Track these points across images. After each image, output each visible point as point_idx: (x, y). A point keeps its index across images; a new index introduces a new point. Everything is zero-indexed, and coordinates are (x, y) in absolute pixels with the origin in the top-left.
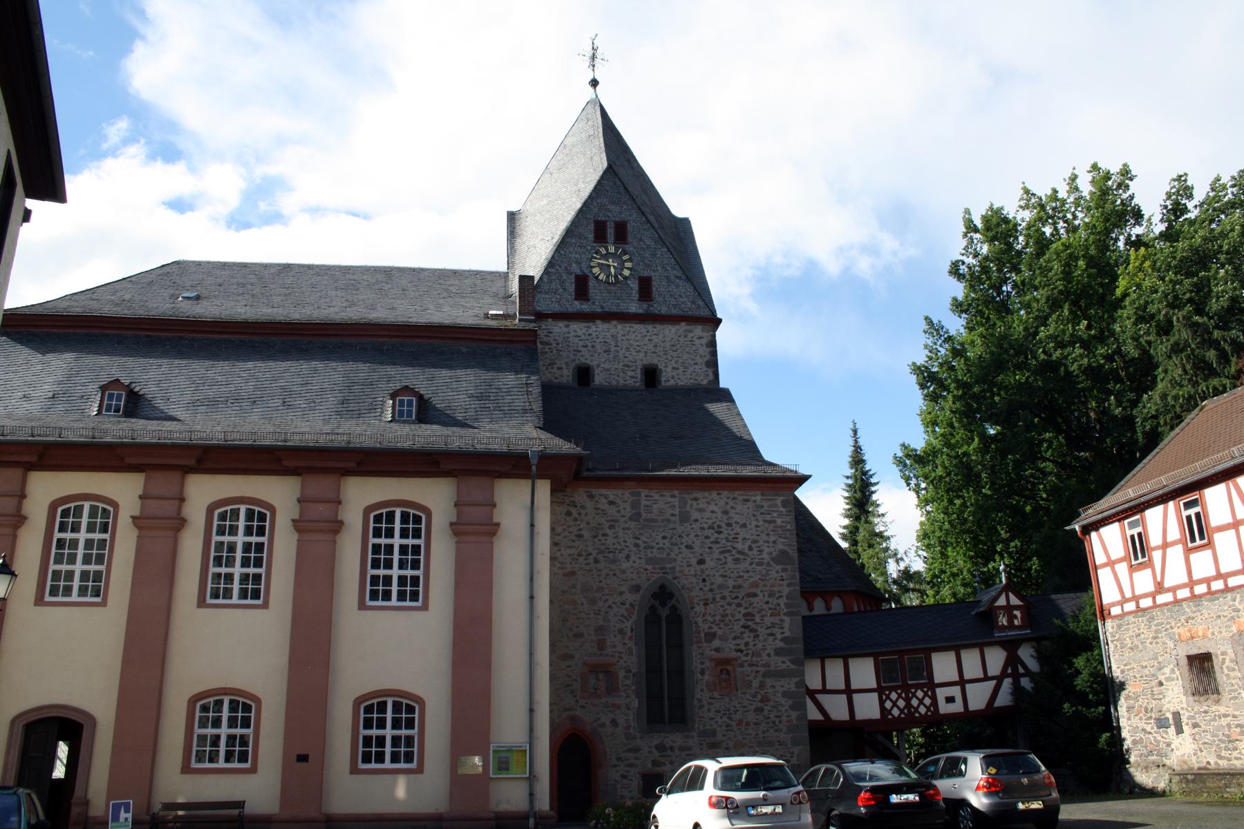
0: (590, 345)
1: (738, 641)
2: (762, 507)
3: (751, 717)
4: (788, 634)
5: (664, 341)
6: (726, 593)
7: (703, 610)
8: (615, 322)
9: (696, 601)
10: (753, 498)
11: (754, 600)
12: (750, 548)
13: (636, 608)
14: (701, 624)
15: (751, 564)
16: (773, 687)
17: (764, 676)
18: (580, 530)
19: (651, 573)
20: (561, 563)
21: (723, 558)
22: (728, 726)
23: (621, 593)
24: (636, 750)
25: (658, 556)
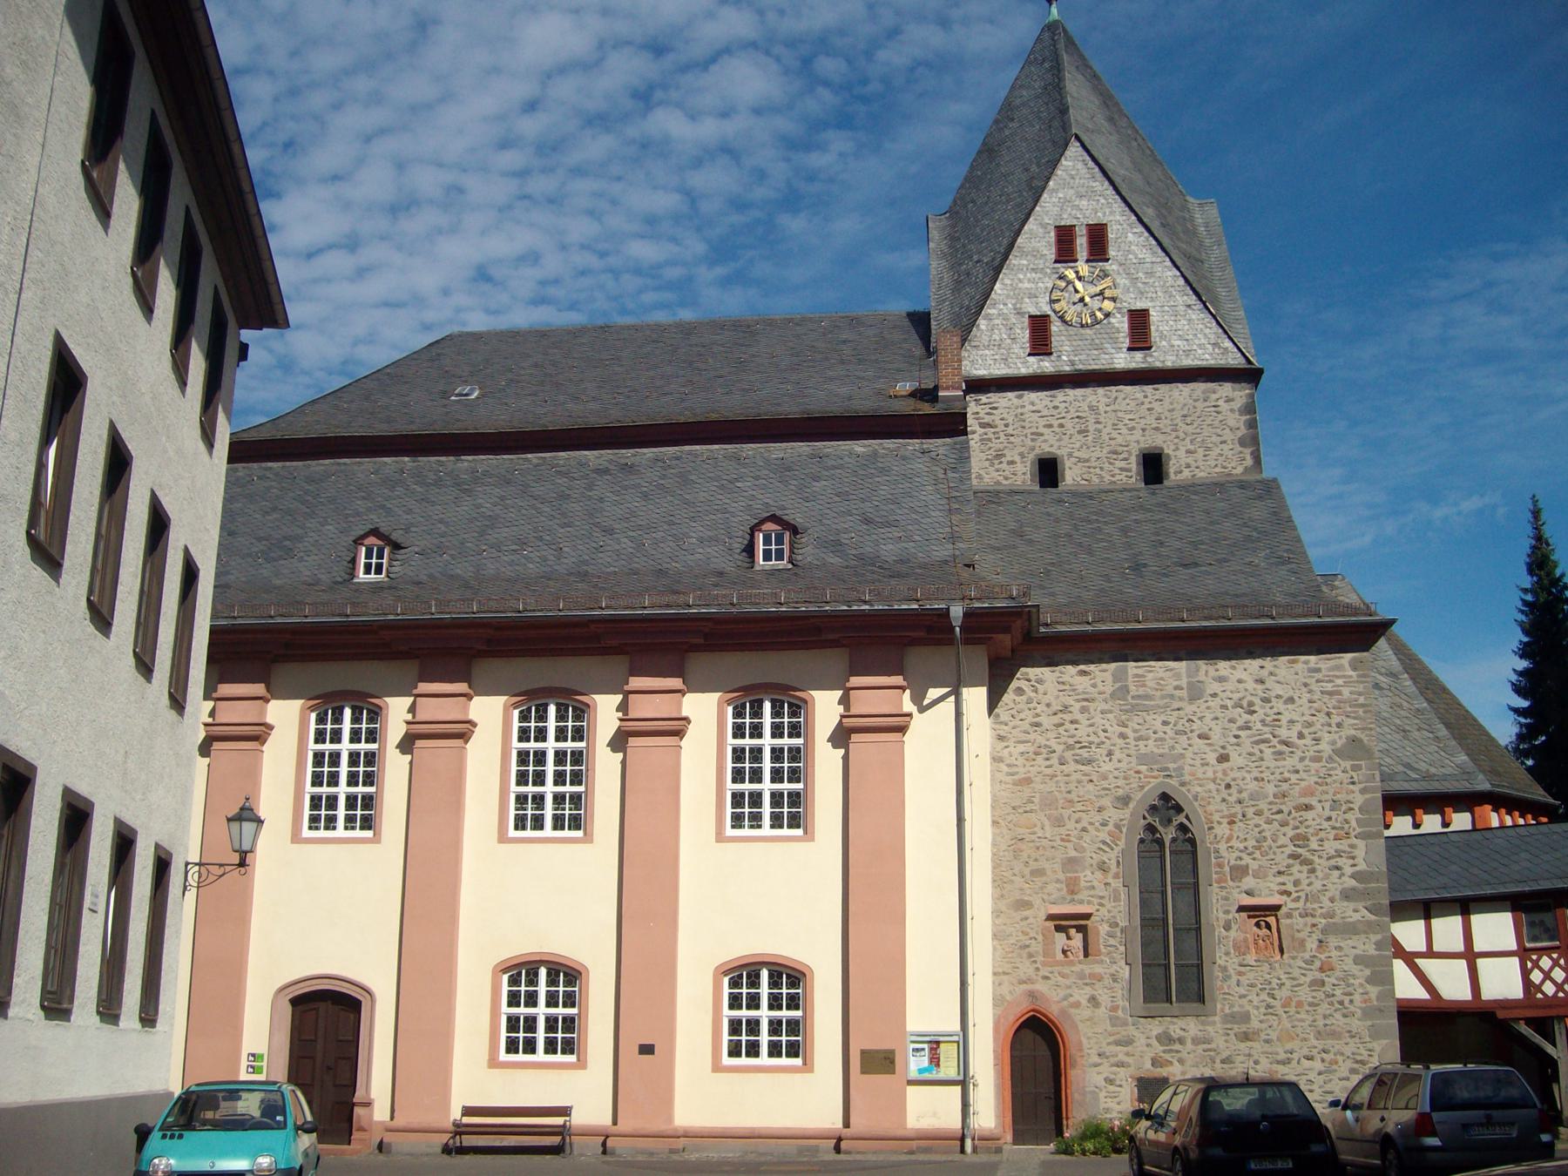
2: (1318, 670)
3: (1305, 994)
4: (1362, 866)
6: (1263, 805)
7: (1228, 832)
9: (1216, 817)
11: (1309, 815)
12: (1301, 736)
13: (1124, 830)
14: (1224, 852)
15: (1302, 759)
16: (1339, 948)
17: (1324, 931)
18: (1038, 715)
22: (1269, 1006)
24: (1128, 1042)
25: (1156, 750)
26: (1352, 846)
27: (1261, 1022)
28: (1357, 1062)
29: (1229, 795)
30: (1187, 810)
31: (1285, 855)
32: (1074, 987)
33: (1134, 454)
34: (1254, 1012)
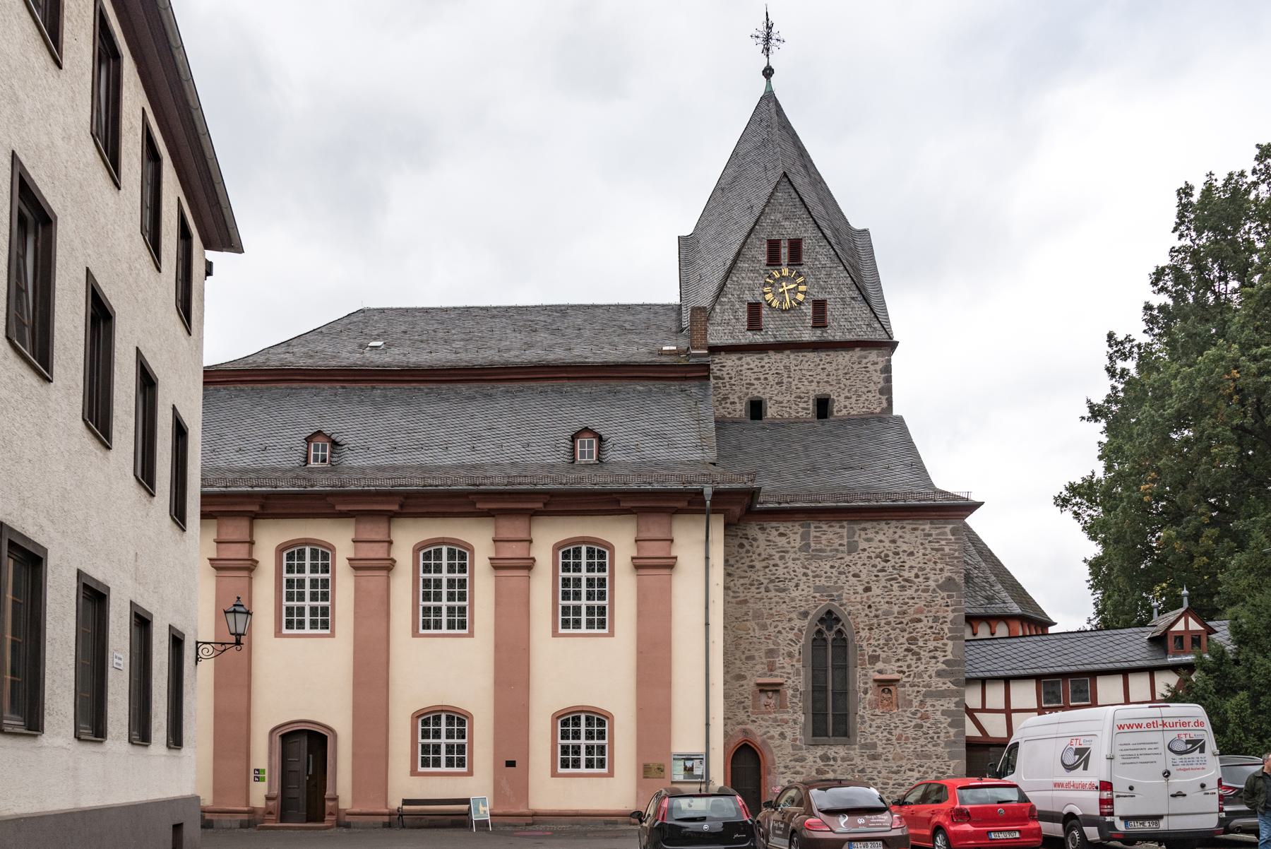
0: (762, 377)
1: (899, 664)
2: (930, 535)
3: (910, 732)
4: (950, 657)
5: (838, 369)
6: (891, 619)
7: (868, 635)
8: (788, 352)
9: (861, 626)
10: (922, 527)
11: (919, 625)
12: (917, 576)
13: (804, 633)
14: (865, 647)
15: (917, 591)
16: (933, 706)
17: (925, 695)
18: (752, 561)
19: (819, 600)
20: (734, 592)
21: (889, 586)
22: (888, 740)
23: (790, 620)
24: (802, 759)
26: (945, 645)
27: (883, 748)
28: (940, 773)
29: (871, 612)
30: (843, 620)
31: (903, 650)
33: (811, 398)
34: (879, 743)
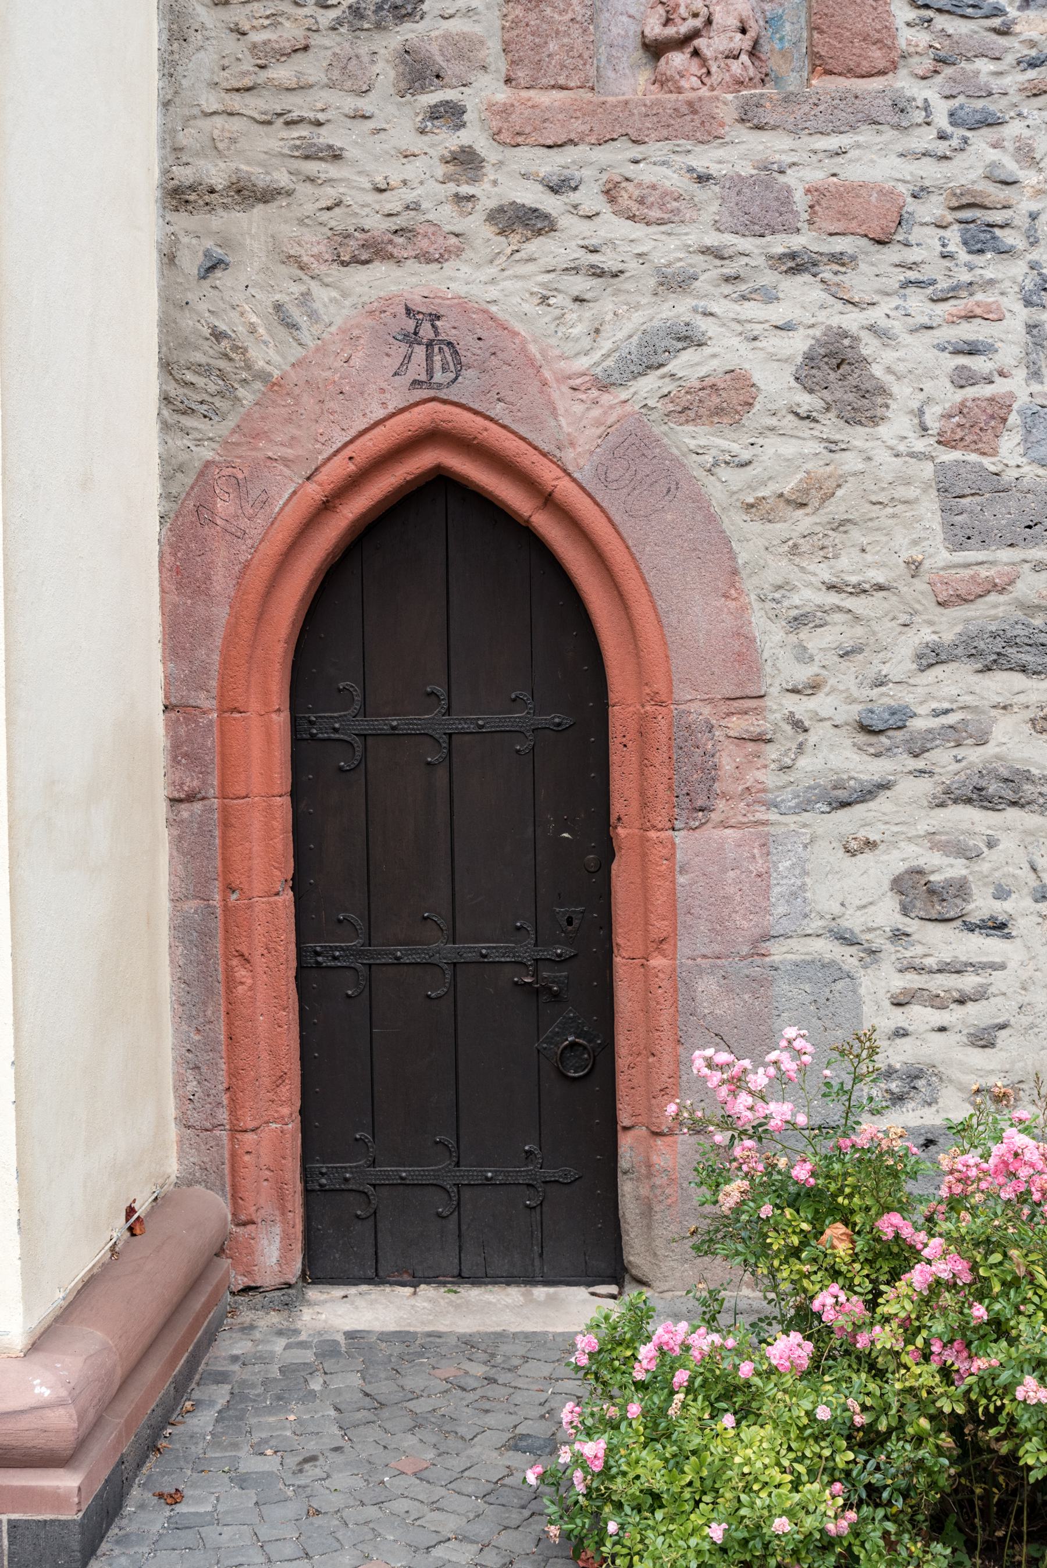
32: (710, 272)
